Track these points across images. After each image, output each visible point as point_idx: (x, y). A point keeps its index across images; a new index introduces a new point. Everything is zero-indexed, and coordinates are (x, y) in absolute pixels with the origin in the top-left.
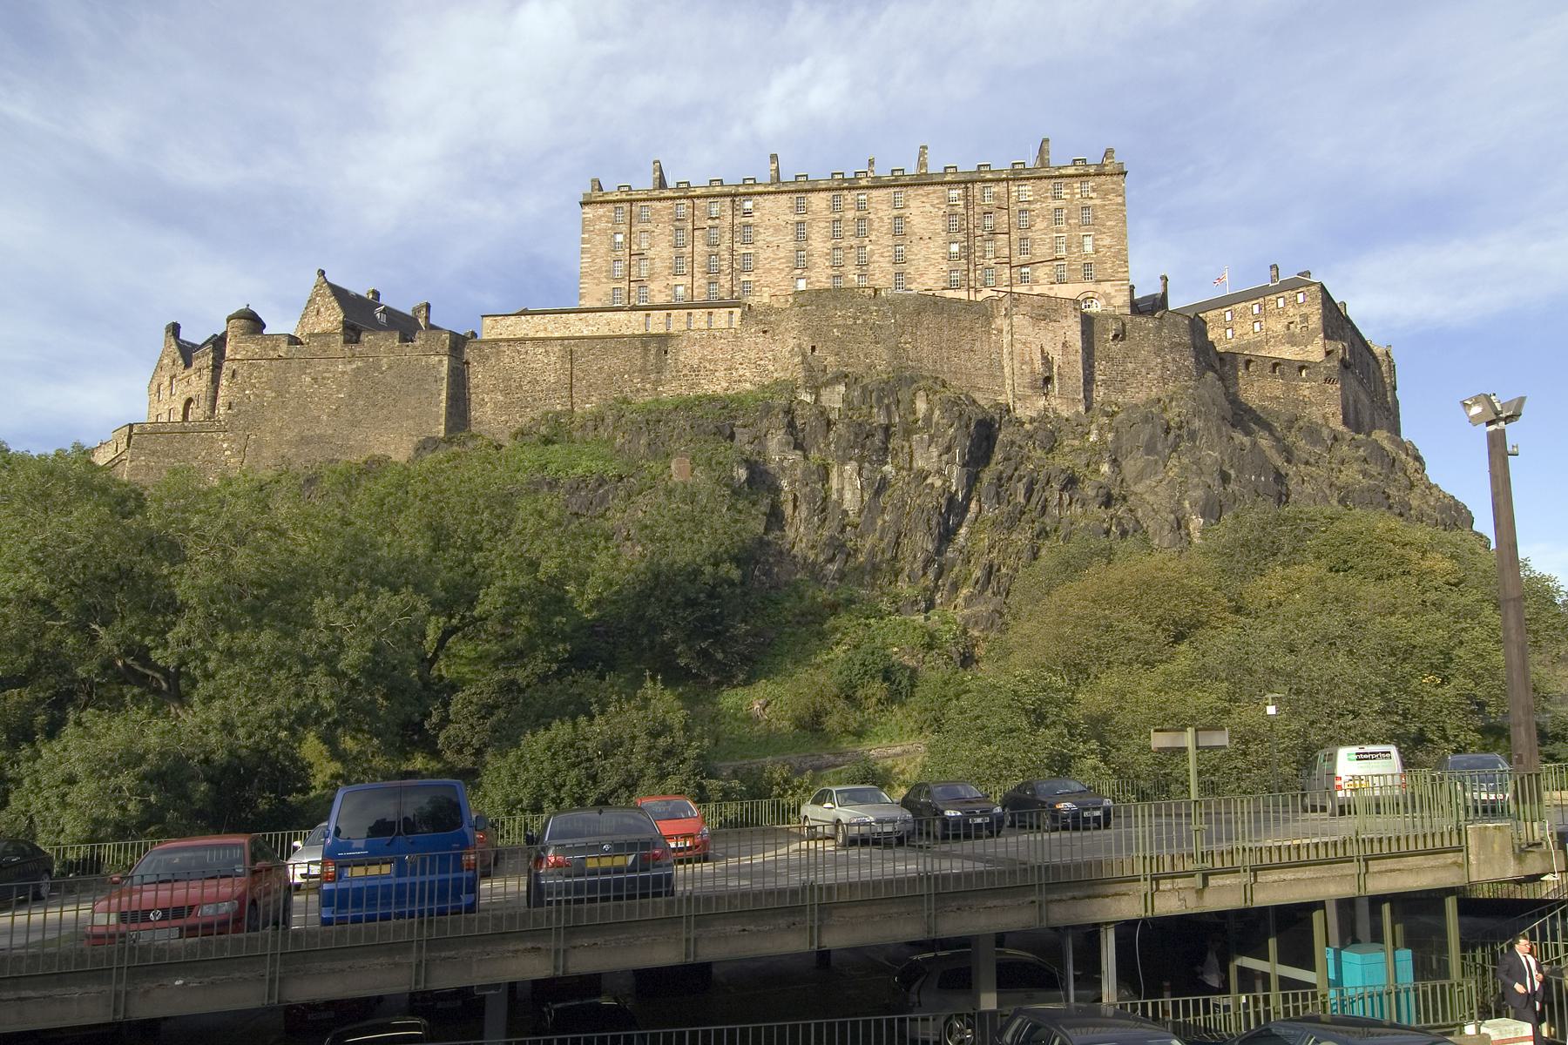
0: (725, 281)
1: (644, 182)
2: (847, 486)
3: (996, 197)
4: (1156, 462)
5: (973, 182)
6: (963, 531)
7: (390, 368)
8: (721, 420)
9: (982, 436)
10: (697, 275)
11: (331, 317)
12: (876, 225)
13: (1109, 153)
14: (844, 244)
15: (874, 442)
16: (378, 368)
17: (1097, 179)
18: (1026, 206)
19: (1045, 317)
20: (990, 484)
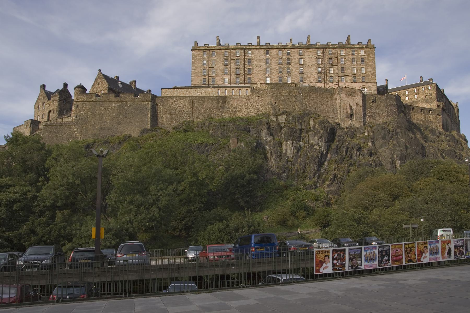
0: (242, 77)
1: (213, 44)
2: (288, 148)
3: (333, 53)
4: (386, 142)
5: (326, 48)
6: (326, 163)
7: (131, 105)
8: (245, 126)
9: (332, 133)
10: (232, 75)
11: (103, 87)
12: (293, 61)
13: (369, 41)
14: (283, 67)
15: (296, 134)
18: (343, 57)
20: (334, 149)
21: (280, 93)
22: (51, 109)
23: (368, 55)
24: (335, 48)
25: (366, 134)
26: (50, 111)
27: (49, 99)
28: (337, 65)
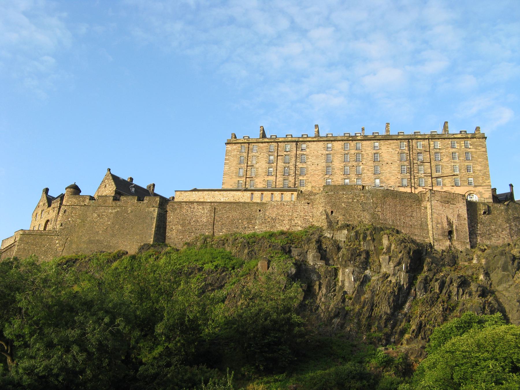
0: (291, 179)
1: (256, 135)
2: (347, 279)
3: (424, 146)
5: (412, 139)
6: (407, 305)
7: (132, 212)
8: (287, 244)
10: (278, 176)
11: (110, 189)
12: (365, 157)
13: (478, 129)
16: (126, 212)
17: (472, 140)
18: (438, 151)
19: (448, 202)
20: (420, 282)
21: (339, 198)
22: (49, 218)
23: (476, 146)
24: (426, 139)
25: (475, 261)
26: (48, 221)
27: (49, 206)
28: (430, 162)
